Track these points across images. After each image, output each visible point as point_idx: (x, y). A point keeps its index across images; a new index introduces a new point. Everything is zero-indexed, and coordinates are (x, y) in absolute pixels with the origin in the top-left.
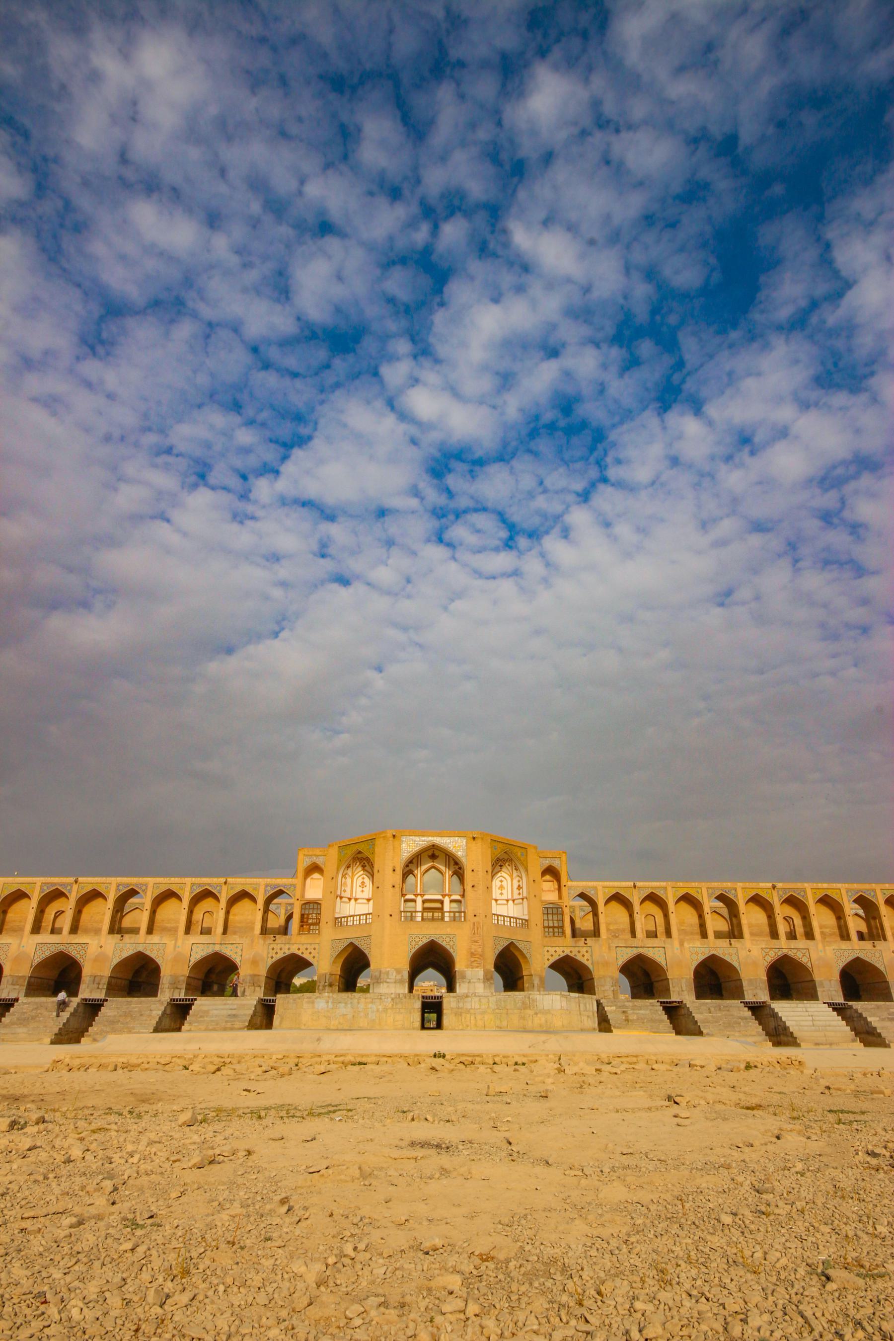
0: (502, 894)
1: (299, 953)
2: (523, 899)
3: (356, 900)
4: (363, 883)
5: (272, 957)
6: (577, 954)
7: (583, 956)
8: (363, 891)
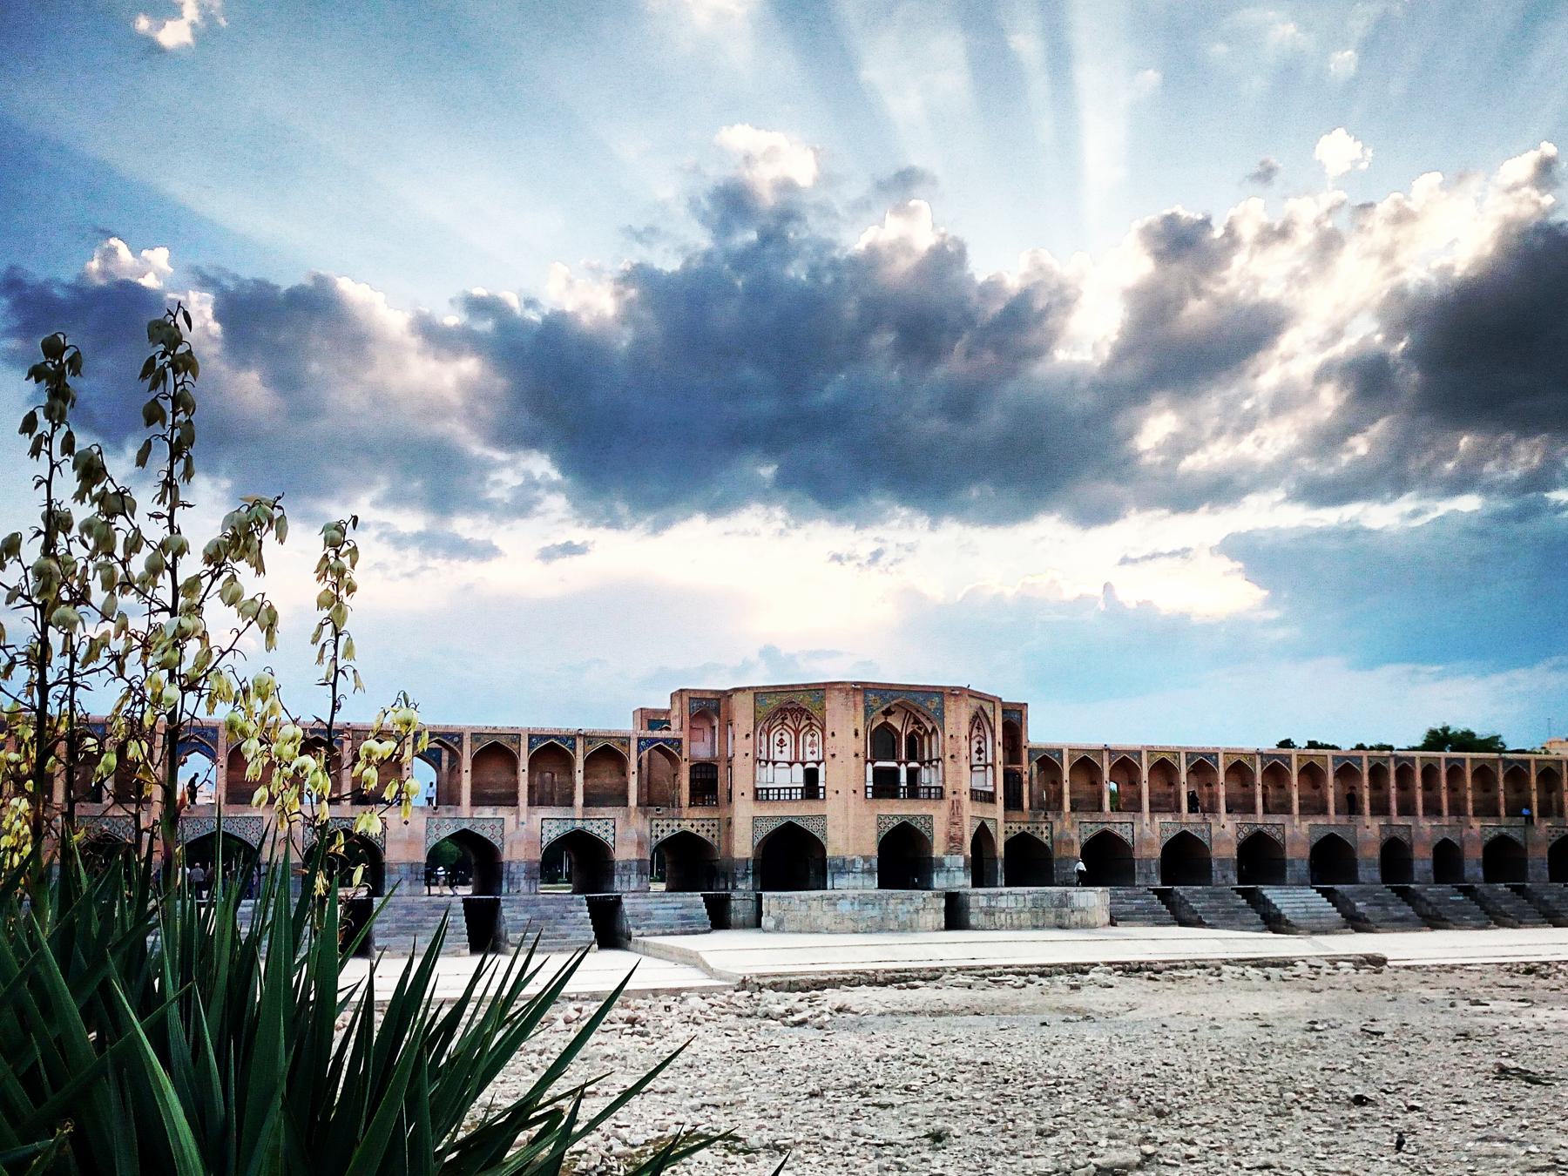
1: (694, 830)
2: (986, 766)
3: (774, 763)
4: (781, 741)
7: (1042, 833)
8: (781, 752)
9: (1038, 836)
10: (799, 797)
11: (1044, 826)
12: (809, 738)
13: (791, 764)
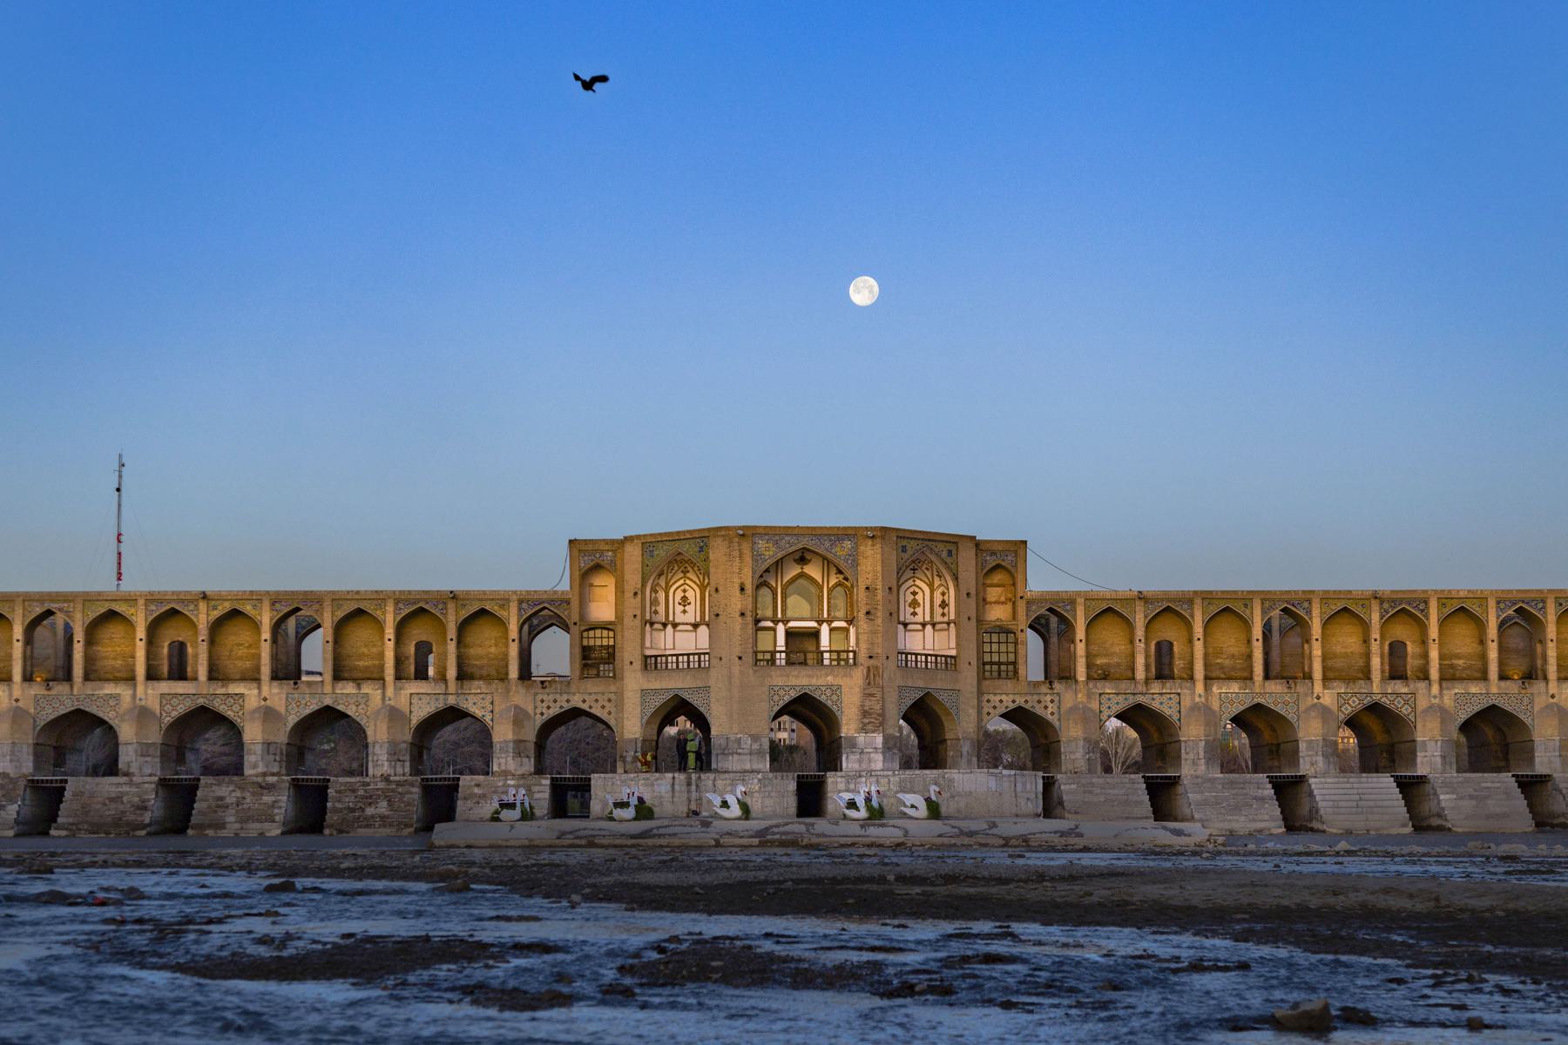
0: (914, 614)
2: (948, 624)
3: (675, 625)
4: (684, 598)
5: (542, 714)
6: (1036, 705)
7: (1046, 707)
8: (684, 612)
9: (1039, 710)
11: (1048, 698)
13: (695, 626)
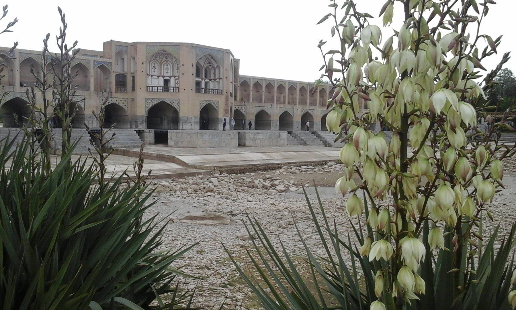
1: (117, 103)
8: (154, 71)
9: (241, 111)
10: (161, 91)
12: (165, 66)
13: (158, 77)
